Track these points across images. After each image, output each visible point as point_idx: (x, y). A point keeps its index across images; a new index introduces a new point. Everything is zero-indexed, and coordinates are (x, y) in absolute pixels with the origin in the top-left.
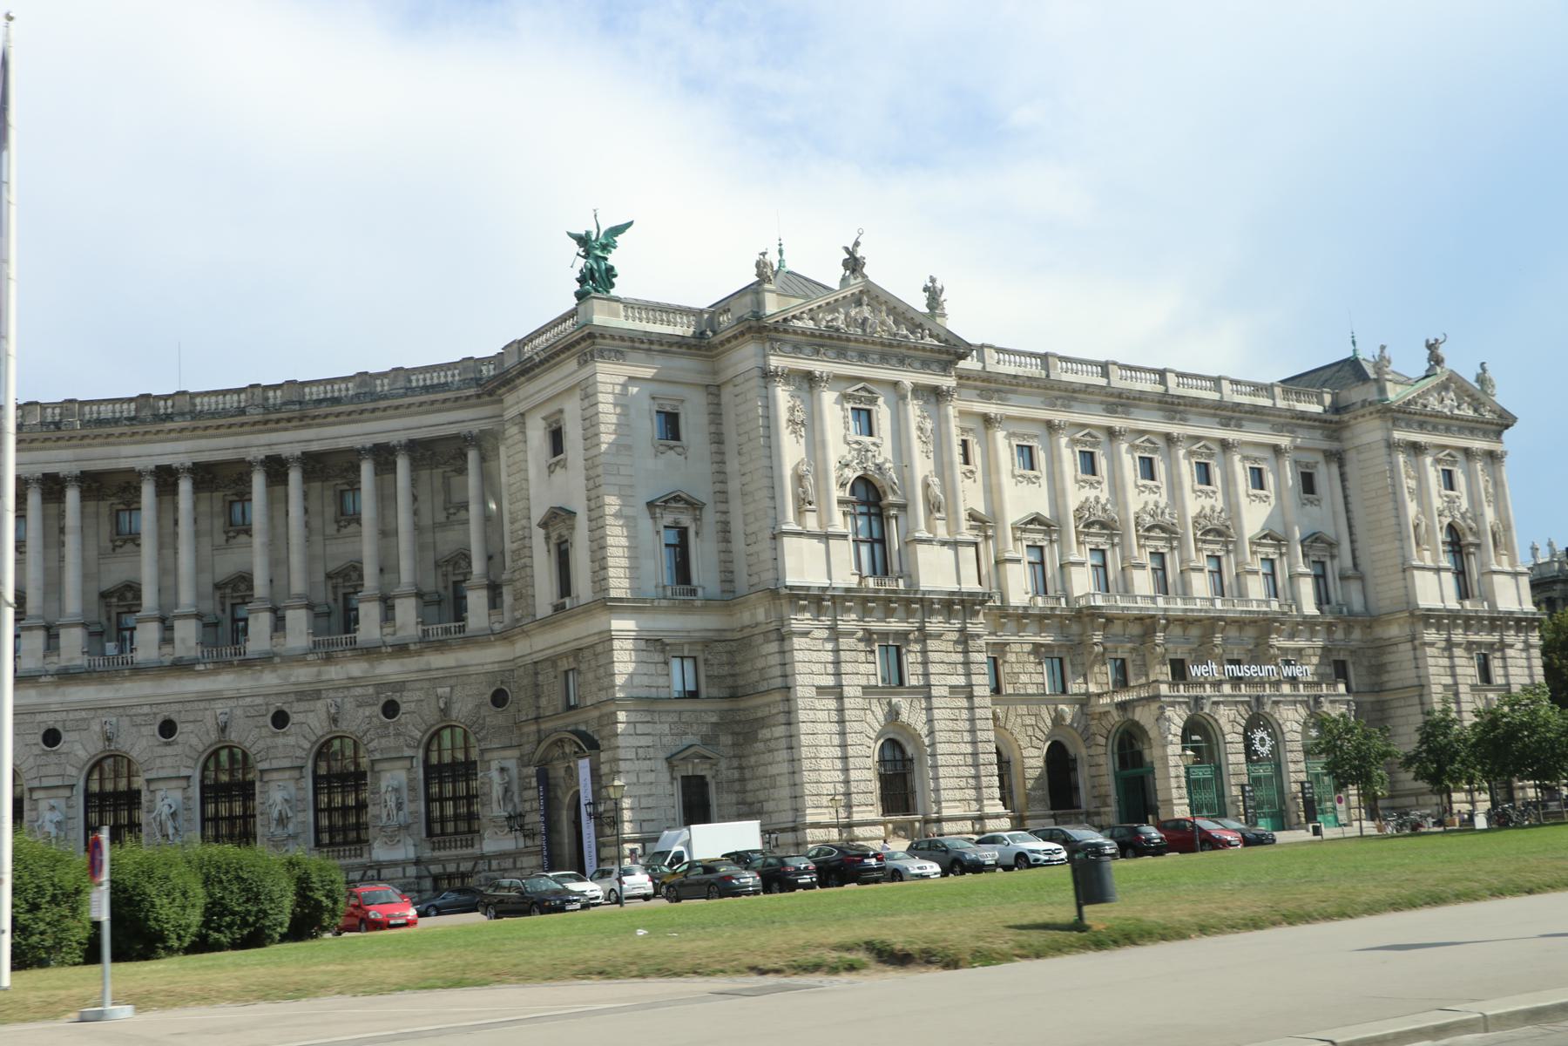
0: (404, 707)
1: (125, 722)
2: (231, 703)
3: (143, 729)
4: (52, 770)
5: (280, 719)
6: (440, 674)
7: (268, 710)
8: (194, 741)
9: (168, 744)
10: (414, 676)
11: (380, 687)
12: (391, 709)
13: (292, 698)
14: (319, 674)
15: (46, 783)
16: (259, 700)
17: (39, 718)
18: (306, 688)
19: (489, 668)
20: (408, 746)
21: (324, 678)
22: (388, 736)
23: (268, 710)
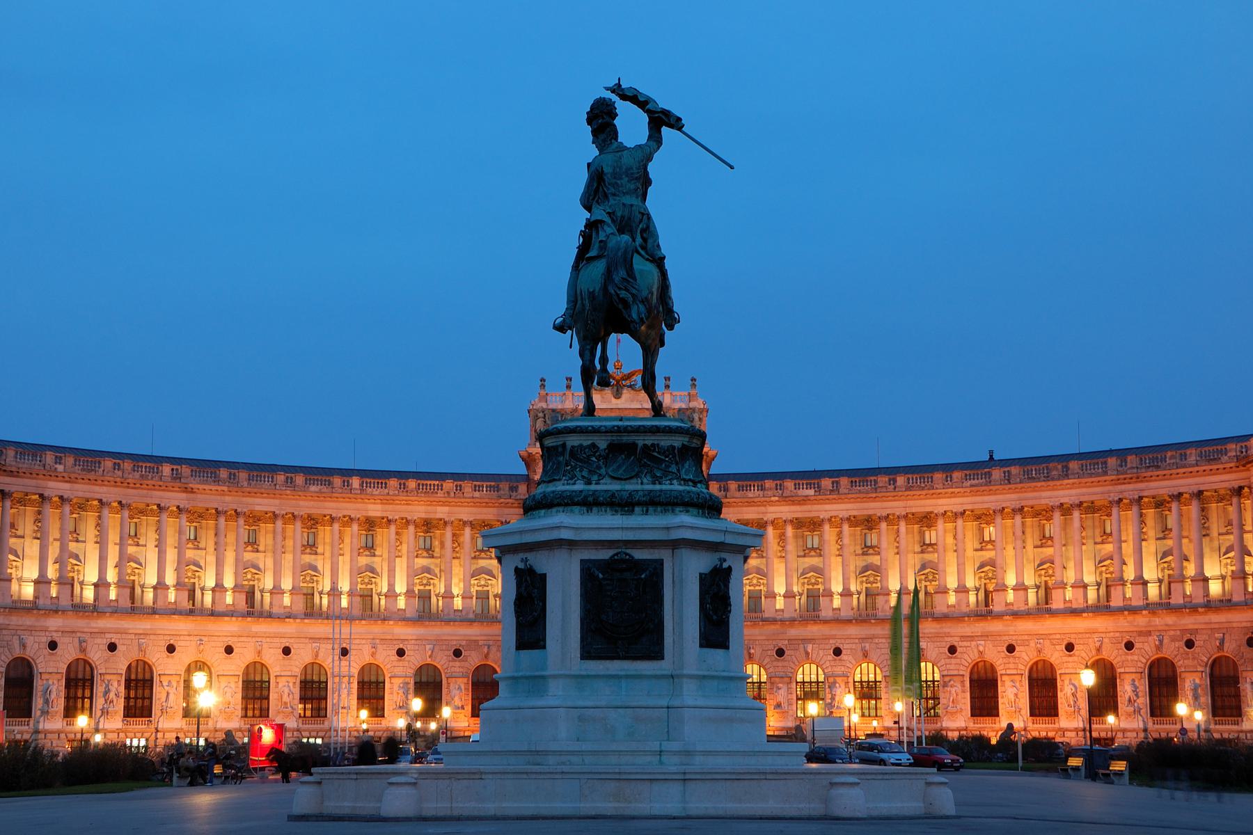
0: (1196, 643)
1: (1047, 643)
2: (1103, 635)
3: (1057, 647)
4: (1011, 666)
5: (1129, 646)
6: (1217, 626)
7: (1122, 640)
8: (1084, 655)
9: (1070, 656)
10: (1203, 626)
11: (1184, 631)
12: (1190, 644)
13: (1135, 634)
14: (1149, 621)
15: (1008, 672)
16: (1118, 634)
17: (1004, 638)
18: (1143, 629)
19: (1244, 624)
20: (1200, 665)
21: (1153, 624)
22: (1189, 658)
23: (1122, 640)
